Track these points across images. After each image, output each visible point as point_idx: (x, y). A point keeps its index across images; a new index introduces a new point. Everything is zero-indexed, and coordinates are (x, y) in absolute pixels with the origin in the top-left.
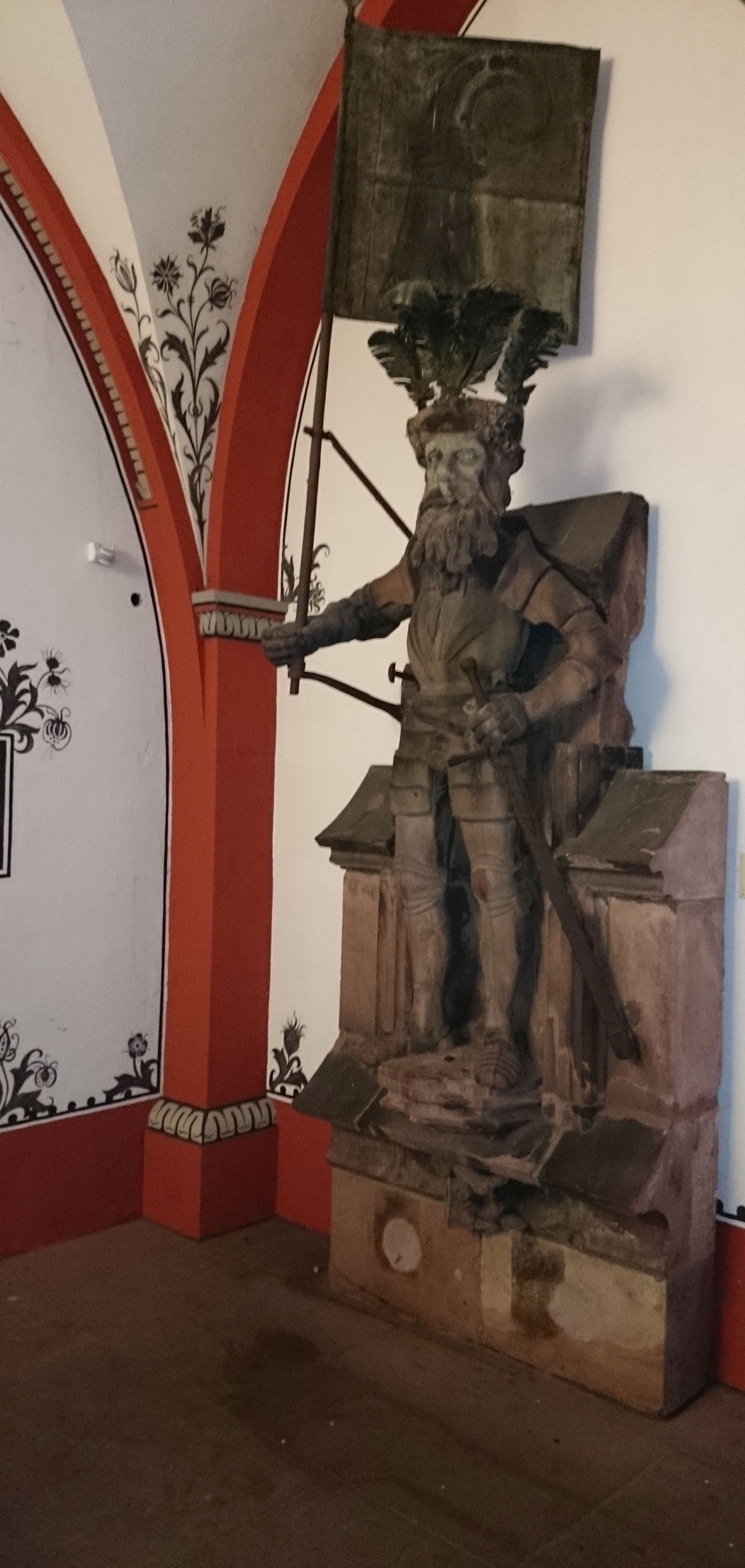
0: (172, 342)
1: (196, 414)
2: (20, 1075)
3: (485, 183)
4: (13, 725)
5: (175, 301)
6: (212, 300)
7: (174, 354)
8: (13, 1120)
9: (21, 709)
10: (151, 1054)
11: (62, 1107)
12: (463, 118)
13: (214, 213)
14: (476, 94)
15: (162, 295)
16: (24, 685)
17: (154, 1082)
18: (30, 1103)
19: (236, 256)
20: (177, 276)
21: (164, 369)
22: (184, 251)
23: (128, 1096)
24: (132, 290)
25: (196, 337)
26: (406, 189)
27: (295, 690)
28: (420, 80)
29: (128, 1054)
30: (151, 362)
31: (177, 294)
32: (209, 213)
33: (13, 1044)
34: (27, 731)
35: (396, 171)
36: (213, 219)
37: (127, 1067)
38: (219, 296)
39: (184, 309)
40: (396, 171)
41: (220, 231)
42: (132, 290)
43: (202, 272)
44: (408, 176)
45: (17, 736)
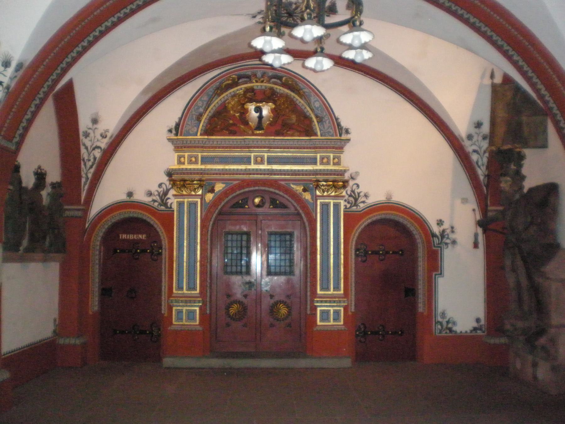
0: (475, 151)
1: (483, 165)
2: (448, 322)
4: (444, 243)
8: (446, 333)
16: (446, 233)
18: (450, 330)
19: (486, 128)
21: (474, 157)
34: (447, 244)
37: (475, 325)
38: (484, 138)
39: (477, 143)
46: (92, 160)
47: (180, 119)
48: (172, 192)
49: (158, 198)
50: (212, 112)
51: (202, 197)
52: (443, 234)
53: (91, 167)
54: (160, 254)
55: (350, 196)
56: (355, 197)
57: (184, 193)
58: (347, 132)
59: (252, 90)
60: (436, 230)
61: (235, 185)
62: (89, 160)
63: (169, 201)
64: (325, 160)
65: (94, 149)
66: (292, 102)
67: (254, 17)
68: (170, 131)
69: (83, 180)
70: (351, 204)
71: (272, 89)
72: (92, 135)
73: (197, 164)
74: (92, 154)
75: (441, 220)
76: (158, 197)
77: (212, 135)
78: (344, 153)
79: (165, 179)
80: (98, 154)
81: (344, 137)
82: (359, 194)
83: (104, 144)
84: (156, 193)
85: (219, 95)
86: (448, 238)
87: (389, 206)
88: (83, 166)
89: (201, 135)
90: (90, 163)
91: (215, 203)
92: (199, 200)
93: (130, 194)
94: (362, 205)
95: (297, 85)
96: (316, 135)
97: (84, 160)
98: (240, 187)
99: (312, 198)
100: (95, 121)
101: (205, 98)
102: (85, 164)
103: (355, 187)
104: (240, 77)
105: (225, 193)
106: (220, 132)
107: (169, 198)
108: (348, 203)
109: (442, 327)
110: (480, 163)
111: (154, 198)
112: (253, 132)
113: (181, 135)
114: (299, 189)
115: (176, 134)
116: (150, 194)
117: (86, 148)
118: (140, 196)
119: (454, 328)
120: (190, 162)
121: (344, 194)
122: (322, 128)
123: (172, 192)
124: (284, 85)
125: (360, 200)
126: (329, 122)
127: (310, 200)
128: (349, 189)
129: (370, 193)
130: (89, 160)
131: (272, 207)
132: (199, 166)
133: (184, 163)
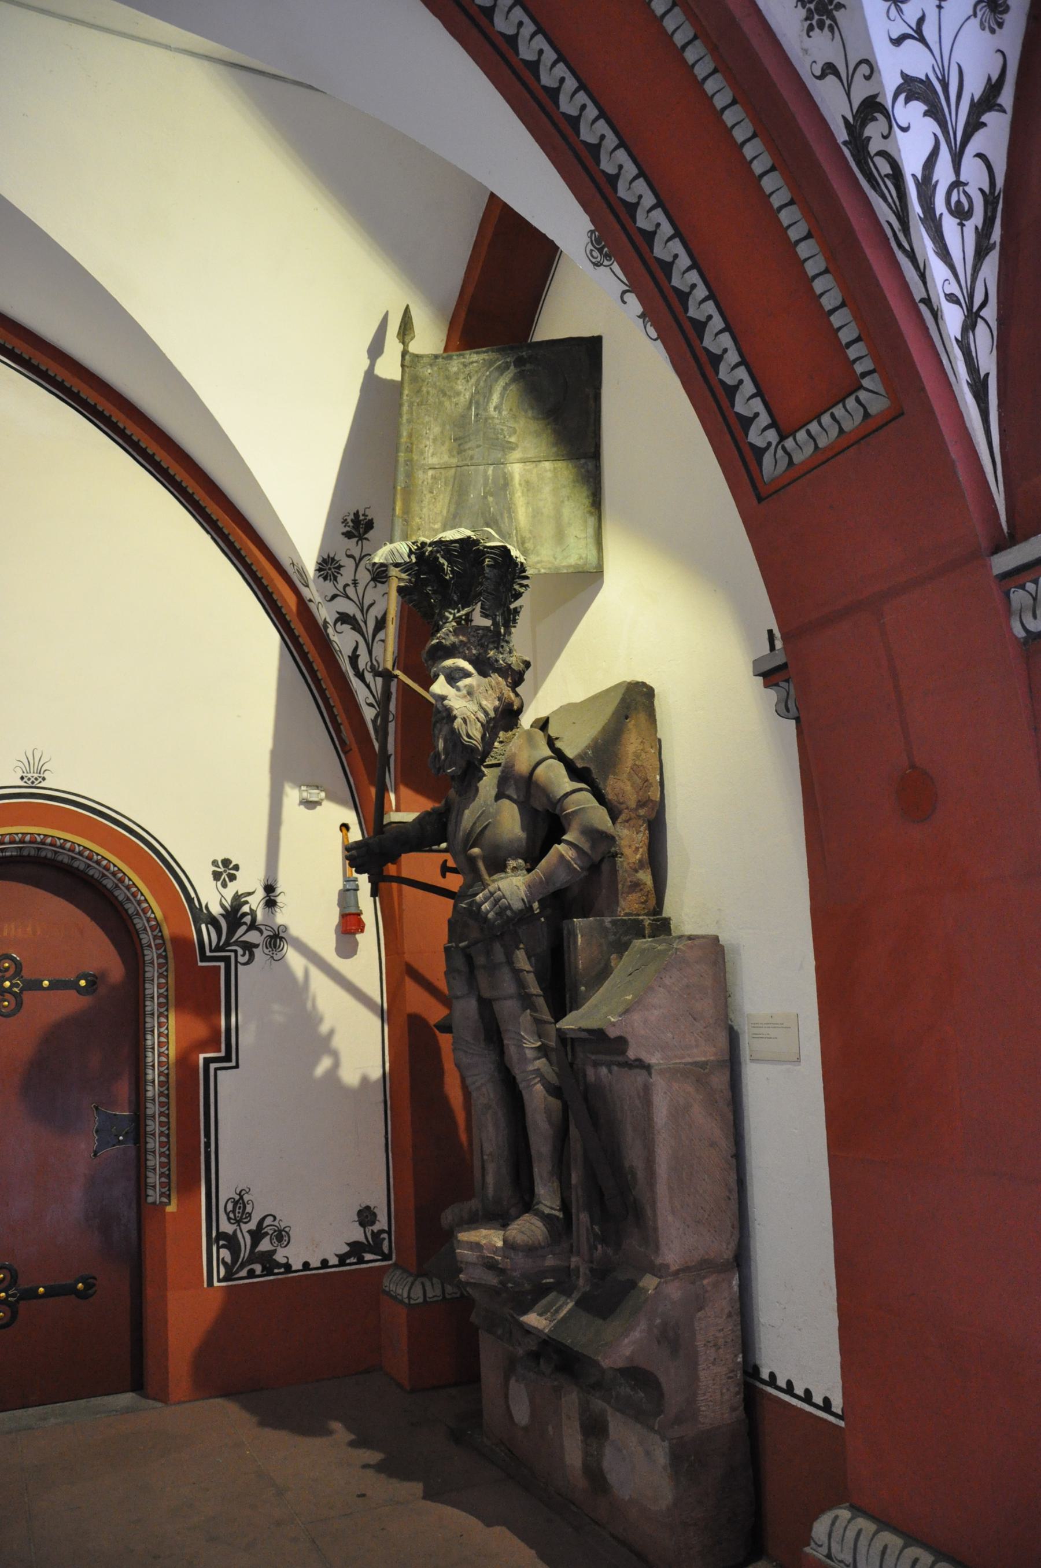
0: (344, 618)
2: (257, 1235)
4: (237, 943)
5: (340, 587)
6: (373, 579)
7: (346, 628)
8: (251, 1274)
9: (244, 928)
11: (297, 1265)
12: (495, 408)
13: (361, 514)
15: (328, 584)
16: (246, 909)
17: (386, 1250)
18: (268, 1262)
20: (340, 567)
21: (343, 640)
22: (343, 547)
23: (361, 1261)
24: (307, 586)
25: (364, 610)
26: (453, 470)
28: (460, 387)
29: (357, 1224)
30: (332, 638)
31: (342, 581)
32: (356, 514)
33: (249, 1209)
35: (446, 458)
36: (361, 518)
37: (357, 1234)
39: (351, 591)
40: (446, 458)
41: (370, 525)
42: (307, 586)
43: (361, 559)
44: (454, 461)
45: (240, 951)
52: (234, 914)
60: (213, 898)
75: (226, 862)
86: (253, 926)
110: (361, 665)
119: (280, 1257)
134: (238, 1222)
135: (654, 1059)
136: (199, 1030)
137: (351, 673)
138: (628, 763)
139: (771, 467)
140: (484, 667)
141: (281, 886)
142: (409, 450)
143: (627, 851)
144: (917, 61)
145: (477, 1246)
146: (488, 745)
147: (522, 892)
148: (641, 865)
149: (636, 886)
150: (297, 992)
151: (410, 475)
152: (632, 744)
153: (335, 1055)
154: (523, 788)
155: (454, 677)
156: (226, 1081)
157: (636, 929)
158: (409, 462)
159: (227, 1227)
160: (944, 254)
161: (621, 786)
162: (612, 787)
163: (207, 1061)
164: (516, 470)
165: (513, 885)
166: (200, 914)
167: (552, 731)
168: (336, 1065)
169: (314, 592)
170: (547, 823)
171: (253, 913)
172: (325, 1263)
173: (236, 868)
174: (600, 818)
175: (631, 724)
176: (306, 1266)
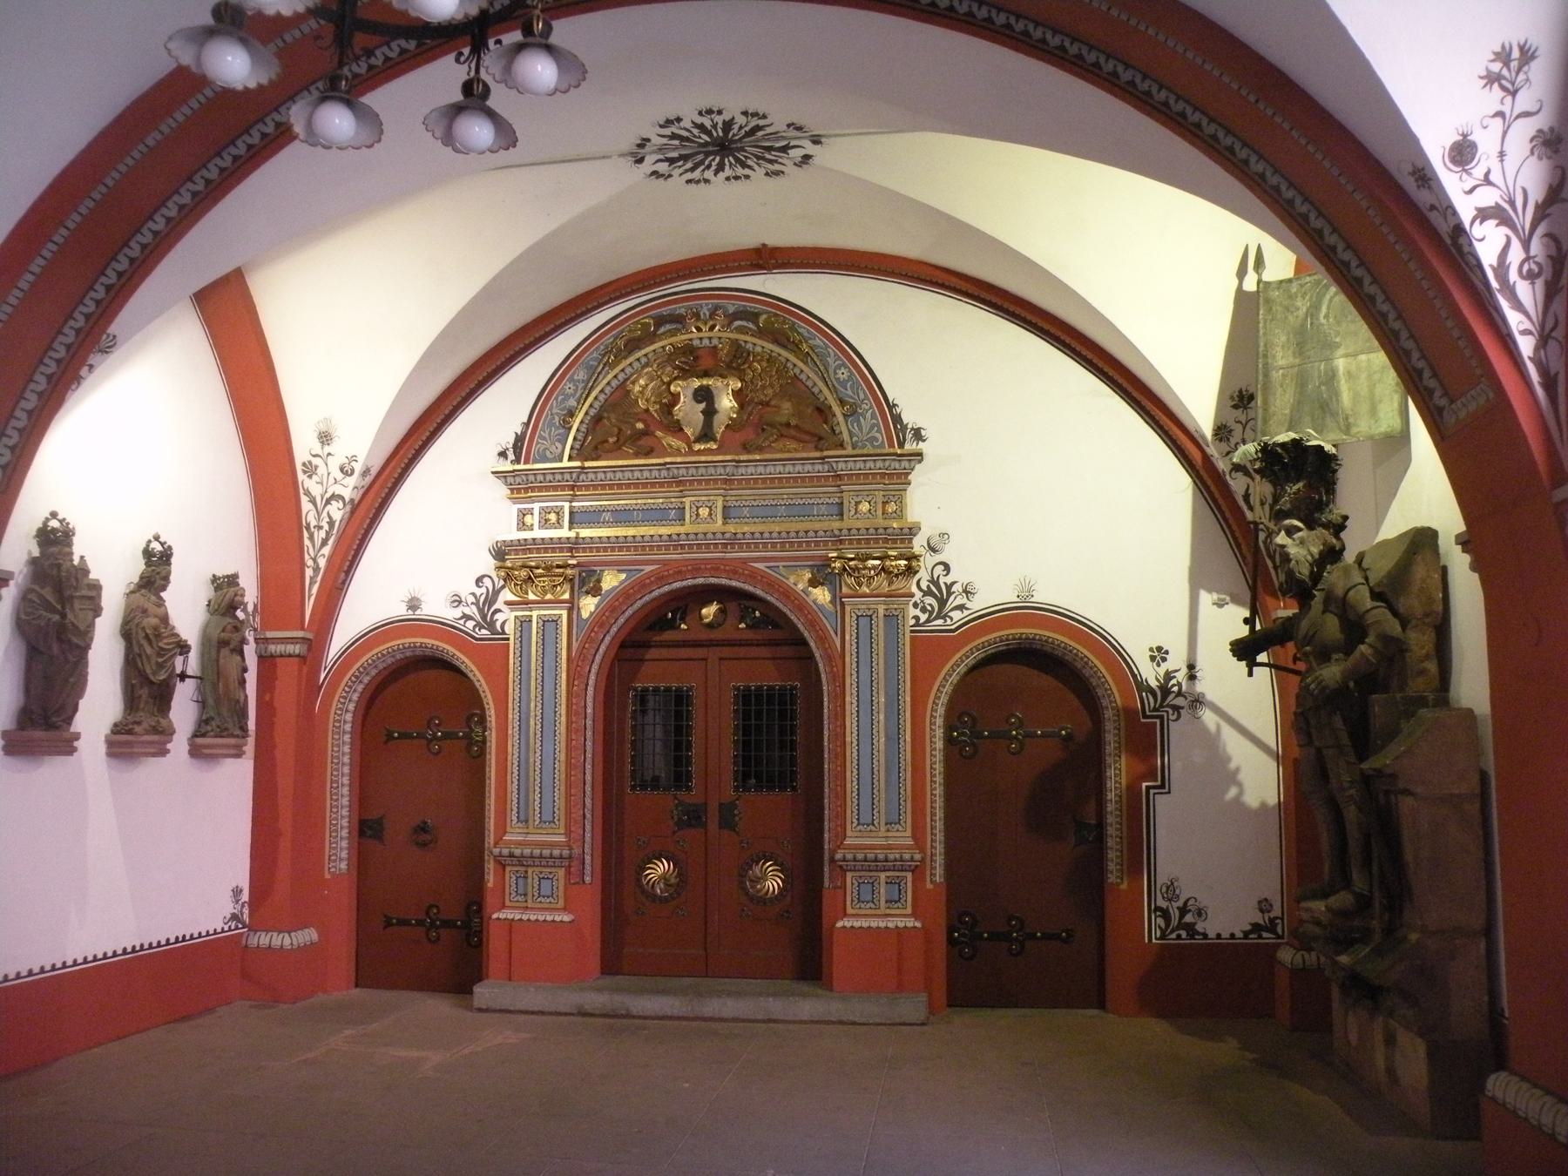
2: (1183, 911)
3: (1341, 351)
7: (1240, 474)
8: (1179, 937)
10: (1276, 912)
14: (1331, 300)
16: (1174, 681)
18: (1190, 928)
22: (1233, 416)
23: (1260, 937)
27: (1250, 674)
28: (1299, 304)
34: (1177, 709)
37: (1258, 918)
41: (1252, 397)
44: (1297, 361)
46: (326, 527)
47: (527, 425)
48: (507, 595)
49: (472, 611)
50: (597, 405)
51: (572, 607)
53: (324, 543)
54: (484, 742)
55: (928, 593)
56: (940, 594)
57: (531, 597)
58: (918, 435)
59: (689, 350)
60: (1150, 674)
61: (649, 575)
62: (320, 528)
63: (500, 617)
64: (864, 507)
65: (328, 502)
66: (782, 370)
67: (640, 161)
68: (503, 454)
69: (309, 572)
70: (931, 613)
71: (735, 344)
72: (322, 470)
73: (561, 527)
74: (325, 514)
75: (1159, 649)
76: (474, 608)
77: (597, 459)
78: (910, 489)
79: (488, 565)
80: (337, 512)
81: (910, 446)
82: (949, 587)
83: (348, 488)
84: (471, 599)
85: (612, 366)
87: (1025, 613)
88: (307, 542)
89: (570, 459)
90: (323, 534)
91: (601, 620)
92: (564, 613)
93: (413, 604)
94: (957, 615)
95: (793, 328)
96: (842, 445)
97: (308, 528)
98: (661, 579)
99: (833, 601)
100: (325, 438)
101: (581, 375)
102: (311, 538)
103: (939, 570)
104: (660, 321)
105: (625, 595)
106: (616, 450)
107: (498, 611)
108: (924, 610)
109: (1167, 925)
111: (467, 611)
112: (690, 447)
113: (526, 462)
114: (799, 581)
115: (517, 461)
116: (457, 601)
117: (313, 501)
118: (437, 607)
119: (1199, 927)
120: (545, 523)
121: (914, 589)
122: (856, 430)
123: (507, 595)
124: (761, 333)
125: (954, 601)
126: (873, 416)
127: (830, 607)
128: (923, 576)
129: (978, 584)
130: (320, 528)
131: (742, 626)
132: (565, 533)
133: (531, 528)
134: (1170, 900)
135: (1419, 790)
136: (1141, 768)
137: (1245, 508)
138: (1415, 589)
139: (1450, 420)
140: (1311, 526)
141: (1201, 664)
142: (1265, 356)
143: (1415, 648)
144: (1487, 197)
145: (1308, 910)
146: (1316, 577)
147: (1338, 676)
148: (1427, 657)
149: (1423, 672)
150: (1212, 743)
151: (1266, 375)
152: (1419, 571)
153: (1240, 785)
154: (1340, 605)
155: (1290, 532)
156: (1162, 803)
157: (1421, 702)
158: (1266, 365)
159: (1162, 903)
160: (1518, 306)
161: (1411, 603)
162: (1403, 604)
163: (1148, 788)
164: (1341, 364)
165: (1332, 672)
166: (1142, 686)
167: (1365, 565)
168: (1241, 792)
169: (1212, 450)
170: (1355, 628)
171: (1179, 684)
172: (1232, 936)
173: (1167, 652)
174: (1394, 627)
175: (1419, 558)
176: (1219, 936)
